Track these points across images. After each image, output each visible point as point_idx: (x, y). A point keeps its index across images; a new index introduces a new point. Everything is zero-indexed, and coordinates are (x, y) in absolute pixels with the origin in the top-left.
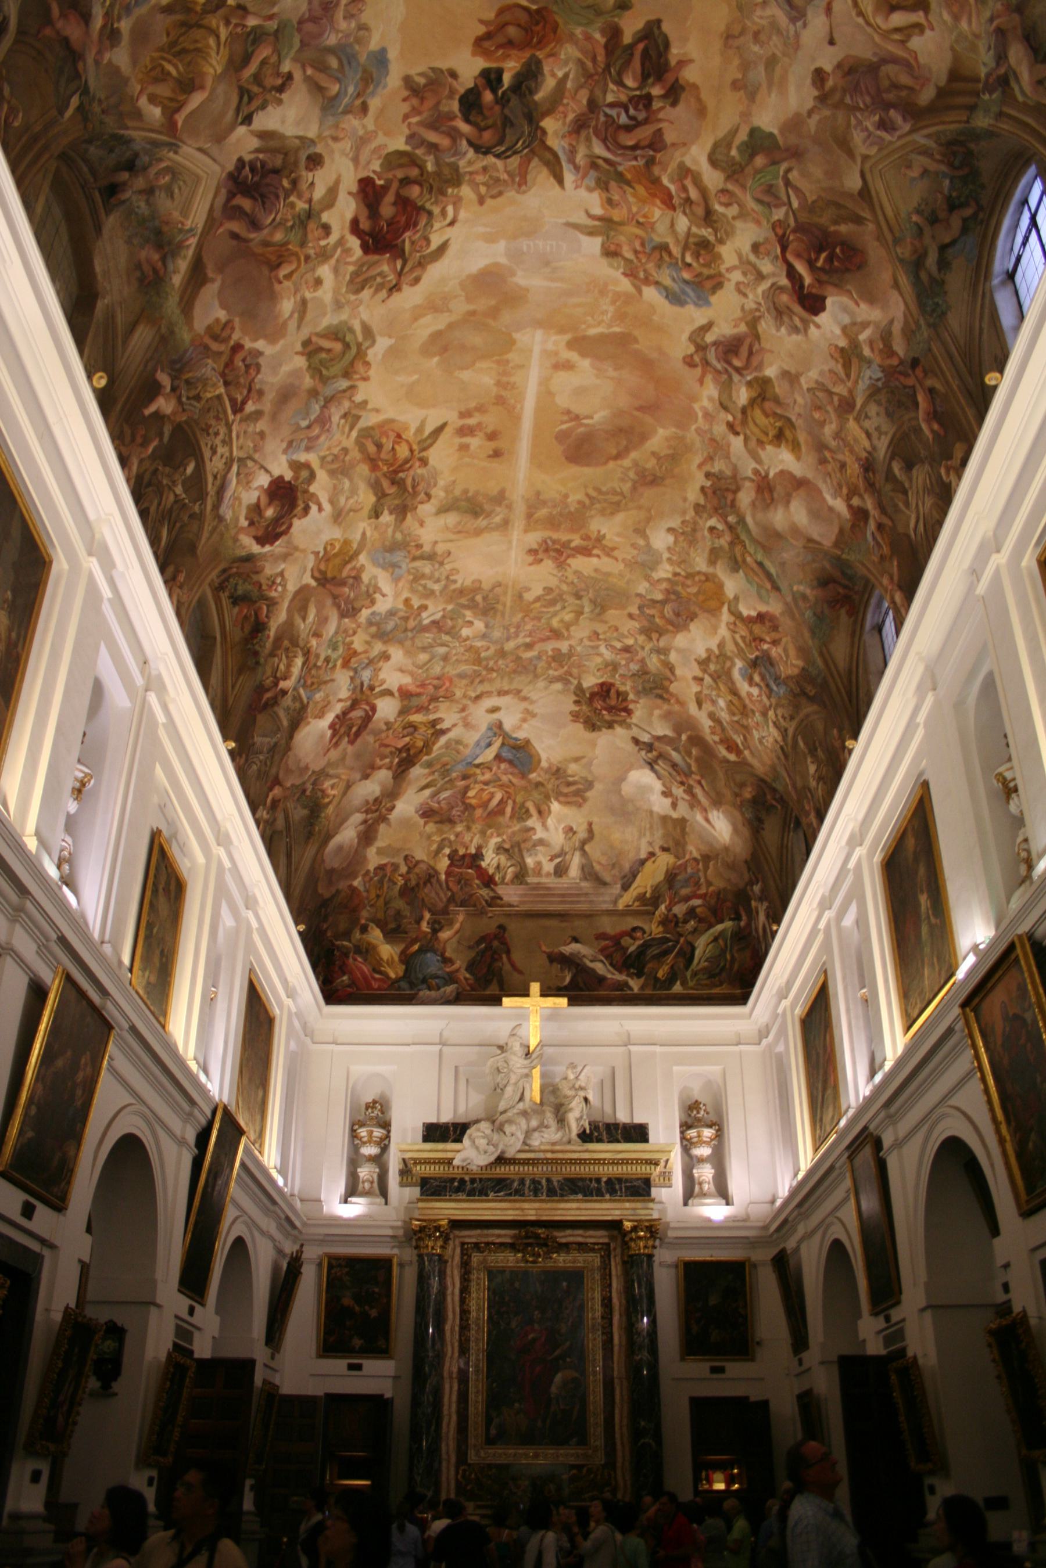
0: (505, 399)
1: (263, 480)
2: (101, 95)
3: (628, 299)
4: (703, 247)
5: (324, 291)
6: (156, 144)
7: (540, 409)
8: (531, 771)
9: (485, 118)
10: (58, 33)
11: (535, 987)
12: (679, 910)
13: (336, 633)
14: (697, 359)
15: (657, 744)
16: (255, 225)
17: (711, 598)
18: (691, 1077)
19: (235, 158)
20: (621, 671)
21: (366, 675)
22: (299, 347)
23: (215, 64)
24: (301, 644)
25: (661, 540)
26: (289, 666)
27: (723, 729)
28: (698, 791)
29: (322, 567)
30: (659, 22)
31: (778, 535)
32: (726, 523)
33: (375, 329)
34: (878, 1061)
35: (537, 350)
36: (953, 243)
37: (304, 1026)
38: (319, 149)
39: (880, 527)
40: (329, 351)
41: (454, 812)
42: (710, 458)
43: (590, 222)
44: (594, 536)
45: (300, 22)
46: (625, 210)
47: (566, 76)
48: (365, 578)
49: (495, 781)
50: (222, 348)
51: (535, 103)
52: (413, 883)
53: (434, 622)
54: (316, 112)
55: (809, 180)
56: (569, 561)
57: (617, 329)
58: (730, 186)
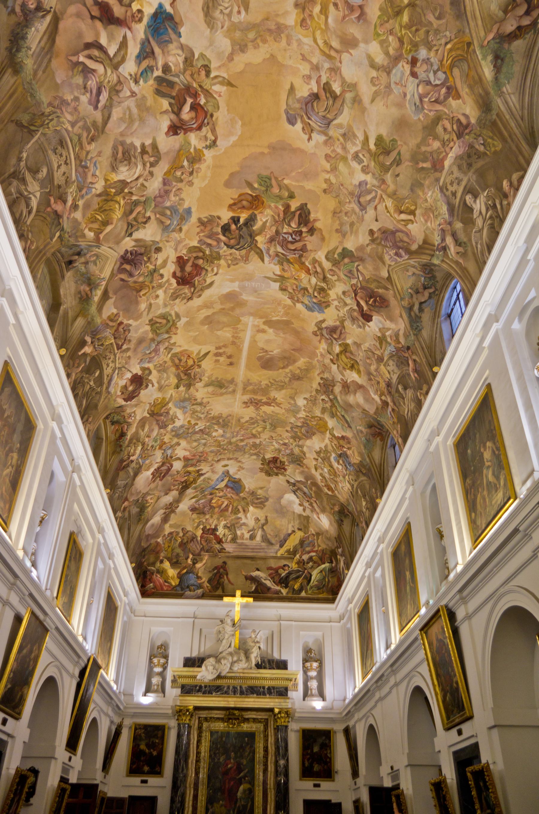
0: (236, 342)
1: (129, 375)
2: (69, 230)
3: (290, 307)
4: (322, 290)
5: (160, 300)
7: (250, 347)
8: (241, 493)
9: (232, 235)
10: (53, 209)
11: (238, 593)
12: (305, 557)
13: (157, 435)
14: (318, 333)
16: (131, 275)
17: (322, 428)
18: (309, 637)
19: (124, 250)
21: (169, 452)
22: (147, 322)
23: (118, 214)
24: (141, 440)
25: (301, 402)
26: (135, 450)
27: (326, 481)
28: (315, 505)
29: (152, 409)
30: (306, 204)
31: (351, 406)
33: (181, 314)
34: (389, 643)
35: (250, 324)
36: (425, 302)
37: (131, 608)
38: (160, 245)
39: (393, 410)
40: (161, 323)
42: (323, 372)
44: (272, 398)
45: (155, 198)
47: (267, 221)
48: (171, 413)
49: (225, 496)
50: (114, 324)
51: (254, 230)
52: (185, 541)
53: (200, 430)
54: (160, 231)
55: (367, 270)
58: (334, 268)
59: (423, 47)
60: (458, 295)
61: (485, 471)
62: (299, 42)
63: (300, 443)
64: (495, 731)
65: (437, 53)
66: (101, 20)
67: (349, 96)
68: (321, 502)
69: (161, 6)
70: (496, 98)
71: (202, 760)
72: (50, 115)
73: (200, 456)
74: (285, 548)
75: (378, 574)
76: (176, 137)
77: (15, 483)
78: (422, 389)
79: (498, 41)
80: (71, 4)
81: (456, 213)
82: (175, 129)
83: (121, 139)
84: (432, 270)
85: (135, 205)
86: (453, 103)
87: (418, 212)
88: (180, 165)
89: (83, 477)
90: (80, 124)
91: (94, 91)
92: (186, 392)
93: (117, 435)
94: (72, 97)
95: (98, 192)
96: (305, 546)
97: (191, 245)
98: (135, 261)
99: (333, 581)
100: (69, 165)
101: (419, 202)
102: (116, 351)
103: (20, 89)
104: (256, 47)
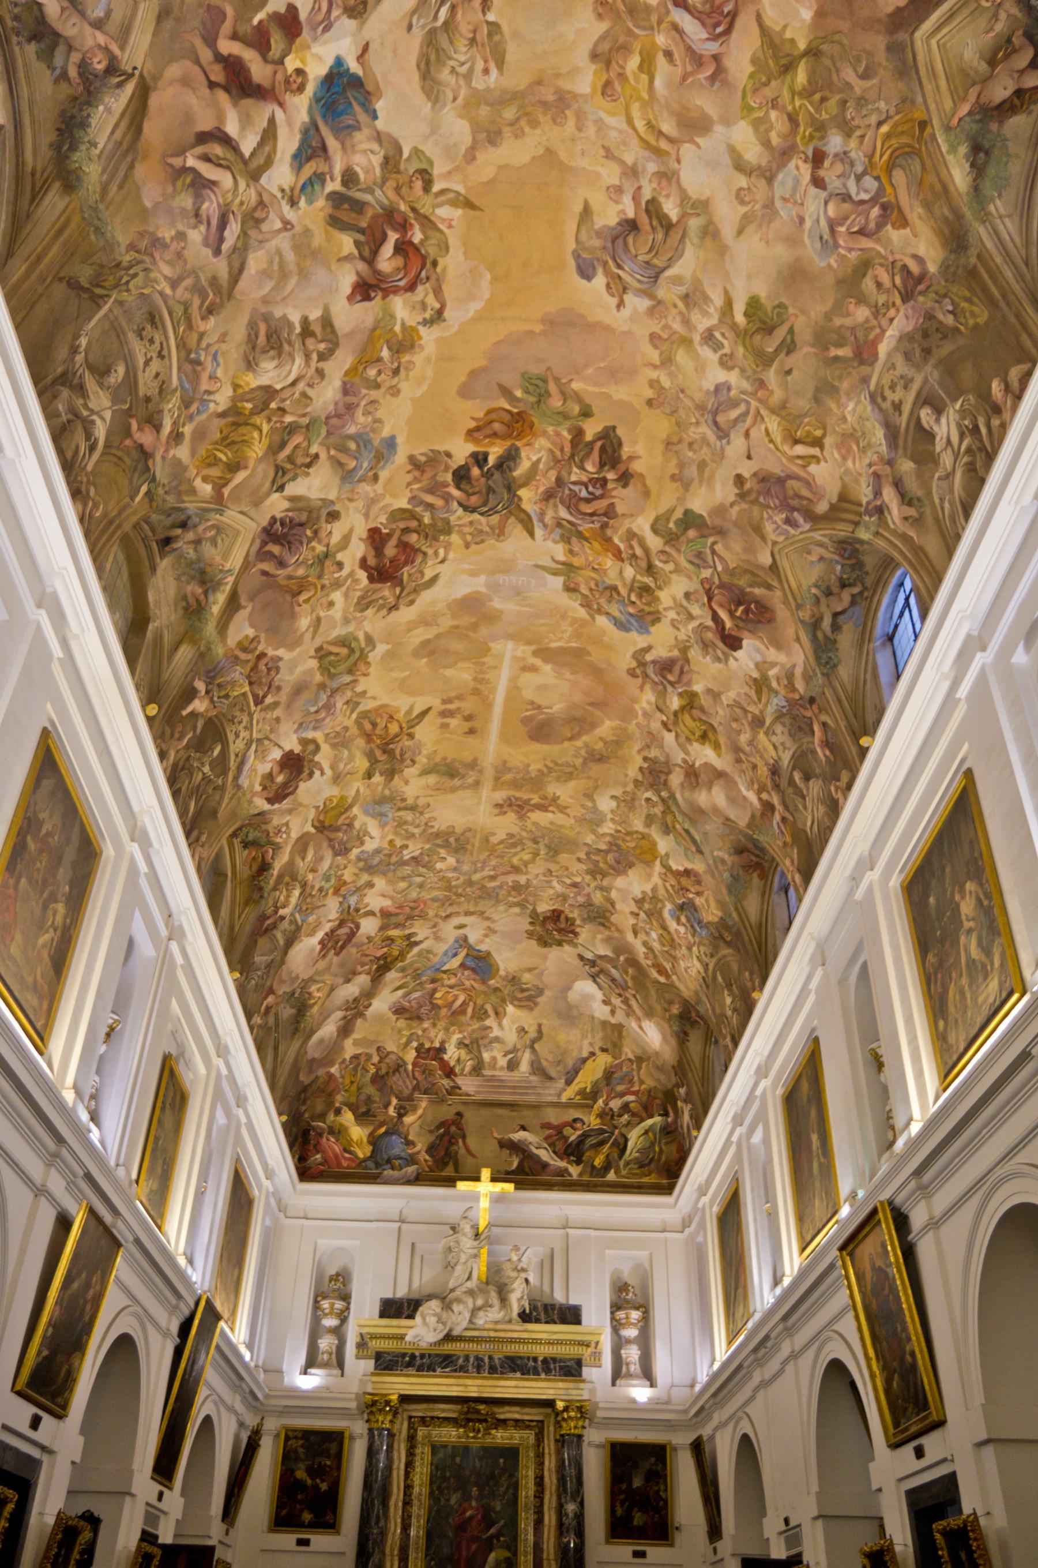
0: (480, 691)
1: (277, 754)
2: (166, 481)
3: (583, 623)
4: (645, 589)
5: (336, 610)
6: (206, 510)
7: (509, 699)
8: (490, 979)
9: (473, 487)
11: (486, 1173)
12: (615, 1104)
13: (330, 868)
14: (638, 672)
15: (599, 962)
16: (281, 564)
17: (647, 854)
18: (623, 1260)
19: (269, 516)
20: (570, 902)
21: (353, 900)
22: (312, 653)
23: (257, 449)
24: (300, 878)
25: (605, 804)
26: (288, 897)
27: (655, 957)
28: (633, 1002)
29: (322, 818)
30: (614, 428)
31: (702, 812)
32: (660, 796)
33: (375, 637)
34: (779, 1274)
35: (508, 656)
37: (279, 1202)
38: (337, 508)
39: (784, 819)
40: (337, 654)
41: (422, 1011)
43: (555, 566)
44: (550, 796)
45: (327, 418)
46: (583, 559)
47: (539, 460)
48: (357, 824)
49: (460, 985)
50: (249, 657)
51: (514, 478)
52: (383, 1071)
54: (337, 481)
55: (731, 552)
57: (574, 645)
58: (667, 549)
59: (834, 130)
60: (907, 599)
61: (963, 939)
62: (600, 124)
63: (605, 883)
65: (861, 142)
66: (226, 89)
67: (694, 224)
68: (646, 998)
69: (339, 62)
70: (975, 224)
71: (415, 1502)
72: (130, 267)
73: (412, 908)
74: (575, 1087)
75: (757, 1138)
76: (366, 304)
77: (59, 961)
78: (838, 780)
79: (978, 117)
80: (172, 60)
81: (901, 442)
82: (364, 290)
83: (263, 309)
84: (857, 551)
85: (289, 433)
86: (894, 235)
87: (828, 441)
88: (375, 356)
89: (189, 949)
90: (188, 282)
91: (214, 222)
92: (385, 786)
93: (255, 868)
94: (173, 233)
95: (220, 409)
96: (614, 1082)
97: (396, 507)
98: (290, 538)
99: (670, 1151)
100: (166, 360)
101: (831, 422)
102: (253, 708)
103: (76, 219)
104: (519, 135)
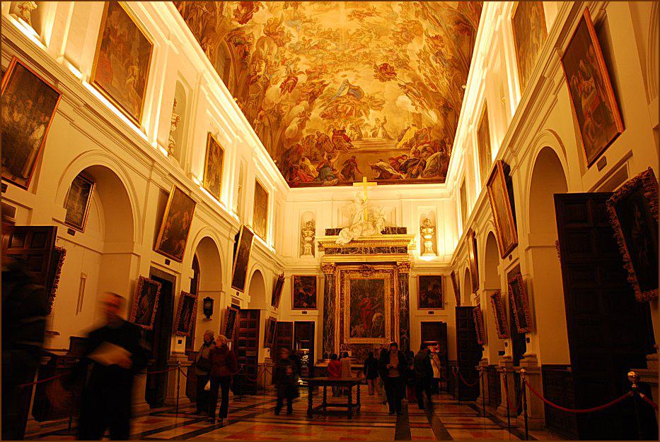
11: (365, 179)
12: (420, 148)
17: (419, 31)
18: (424, 210)
21: (292, 67)
27: (430, 80)
28: (424, 103)
29: (268, 29)
48: (286, 31)
56: (364, 18)
64: (530, 251)
71: (345, 299)
74: (402, 142)
77: (141, 89)
